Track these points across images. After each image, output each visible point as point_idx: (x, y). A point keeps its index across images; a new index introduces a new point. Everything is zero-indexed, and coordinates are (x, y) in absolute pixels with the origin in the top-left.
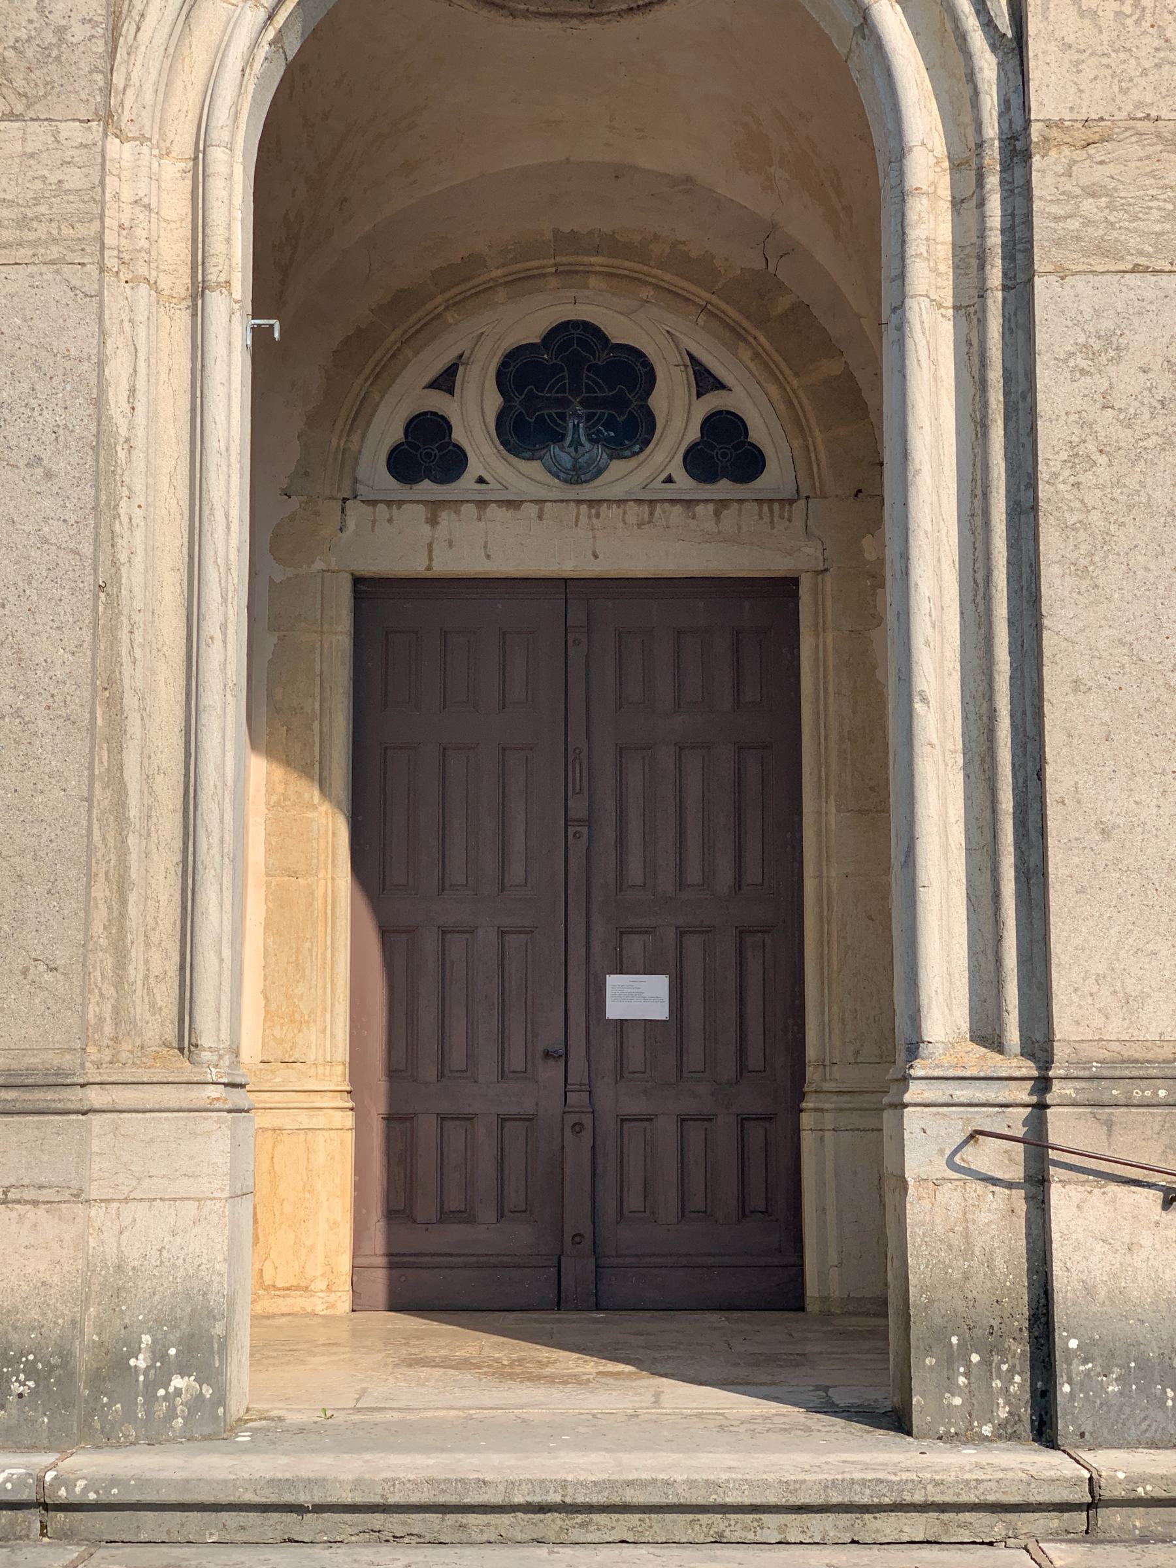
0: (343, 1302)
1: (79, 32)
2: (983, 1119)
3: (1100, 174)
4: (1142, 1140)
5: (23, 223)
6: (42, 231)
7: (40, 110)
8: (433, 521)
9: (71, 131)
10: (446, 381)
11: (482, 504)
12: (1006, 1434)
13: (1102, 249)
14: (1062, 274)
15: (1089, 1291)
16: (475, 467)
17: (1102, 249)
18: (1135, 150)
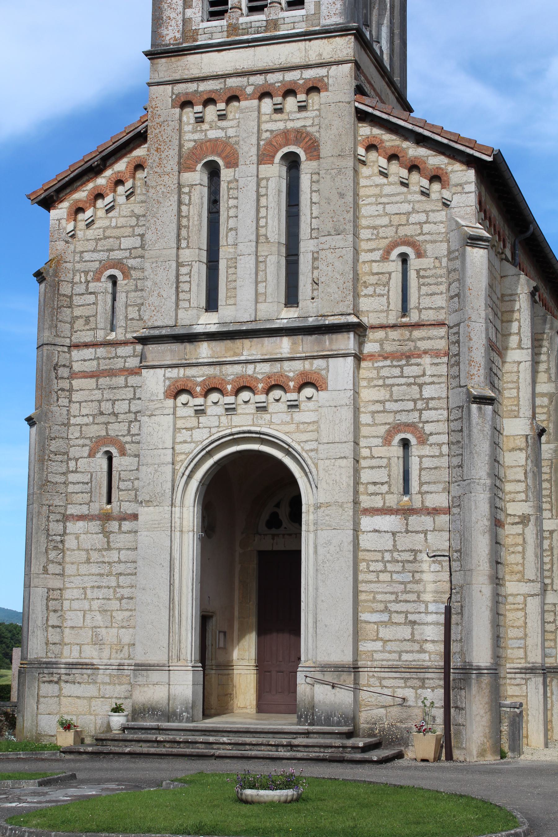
0: (254, 710)
1: (167, 491)
2: (308, 674)
3: (328, 512)
4: (329, 677)
5: (159, 524)
6: (162, 525)
7: (161, 504)
8: (273, 539)
9: (166, 508)
10: (278, 505)
11: (284, 535)
12: (310, 725)
13: (329, 525)
14: (322, 530)
15: (320, 701)
16: (284, 525)
17: (329, 525)
18: (334, 508)
